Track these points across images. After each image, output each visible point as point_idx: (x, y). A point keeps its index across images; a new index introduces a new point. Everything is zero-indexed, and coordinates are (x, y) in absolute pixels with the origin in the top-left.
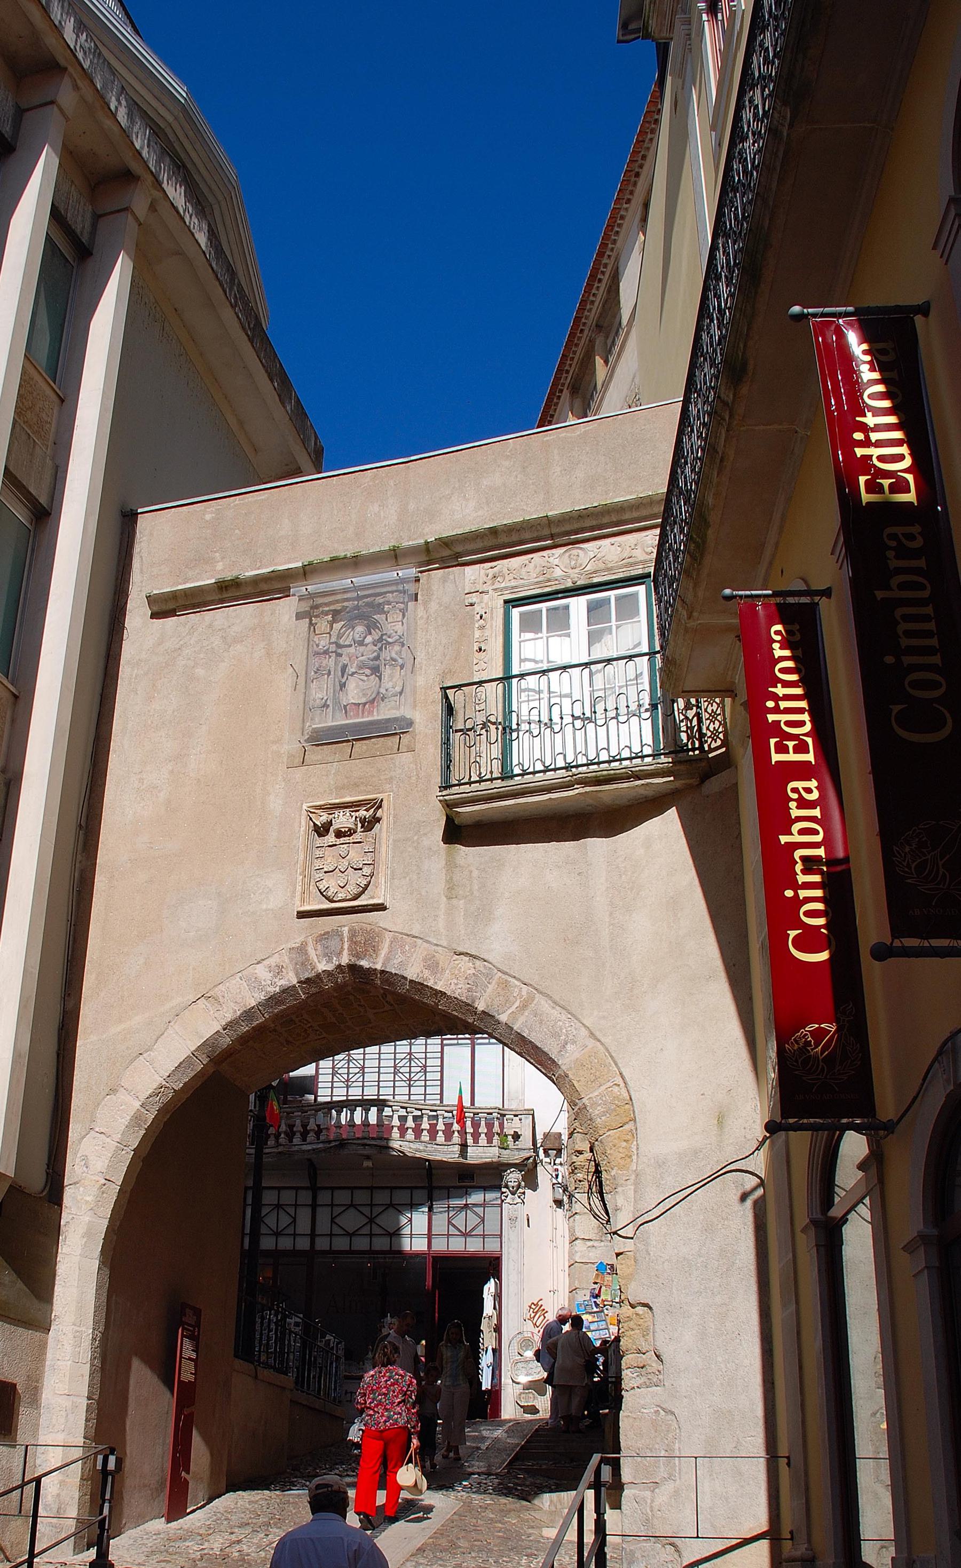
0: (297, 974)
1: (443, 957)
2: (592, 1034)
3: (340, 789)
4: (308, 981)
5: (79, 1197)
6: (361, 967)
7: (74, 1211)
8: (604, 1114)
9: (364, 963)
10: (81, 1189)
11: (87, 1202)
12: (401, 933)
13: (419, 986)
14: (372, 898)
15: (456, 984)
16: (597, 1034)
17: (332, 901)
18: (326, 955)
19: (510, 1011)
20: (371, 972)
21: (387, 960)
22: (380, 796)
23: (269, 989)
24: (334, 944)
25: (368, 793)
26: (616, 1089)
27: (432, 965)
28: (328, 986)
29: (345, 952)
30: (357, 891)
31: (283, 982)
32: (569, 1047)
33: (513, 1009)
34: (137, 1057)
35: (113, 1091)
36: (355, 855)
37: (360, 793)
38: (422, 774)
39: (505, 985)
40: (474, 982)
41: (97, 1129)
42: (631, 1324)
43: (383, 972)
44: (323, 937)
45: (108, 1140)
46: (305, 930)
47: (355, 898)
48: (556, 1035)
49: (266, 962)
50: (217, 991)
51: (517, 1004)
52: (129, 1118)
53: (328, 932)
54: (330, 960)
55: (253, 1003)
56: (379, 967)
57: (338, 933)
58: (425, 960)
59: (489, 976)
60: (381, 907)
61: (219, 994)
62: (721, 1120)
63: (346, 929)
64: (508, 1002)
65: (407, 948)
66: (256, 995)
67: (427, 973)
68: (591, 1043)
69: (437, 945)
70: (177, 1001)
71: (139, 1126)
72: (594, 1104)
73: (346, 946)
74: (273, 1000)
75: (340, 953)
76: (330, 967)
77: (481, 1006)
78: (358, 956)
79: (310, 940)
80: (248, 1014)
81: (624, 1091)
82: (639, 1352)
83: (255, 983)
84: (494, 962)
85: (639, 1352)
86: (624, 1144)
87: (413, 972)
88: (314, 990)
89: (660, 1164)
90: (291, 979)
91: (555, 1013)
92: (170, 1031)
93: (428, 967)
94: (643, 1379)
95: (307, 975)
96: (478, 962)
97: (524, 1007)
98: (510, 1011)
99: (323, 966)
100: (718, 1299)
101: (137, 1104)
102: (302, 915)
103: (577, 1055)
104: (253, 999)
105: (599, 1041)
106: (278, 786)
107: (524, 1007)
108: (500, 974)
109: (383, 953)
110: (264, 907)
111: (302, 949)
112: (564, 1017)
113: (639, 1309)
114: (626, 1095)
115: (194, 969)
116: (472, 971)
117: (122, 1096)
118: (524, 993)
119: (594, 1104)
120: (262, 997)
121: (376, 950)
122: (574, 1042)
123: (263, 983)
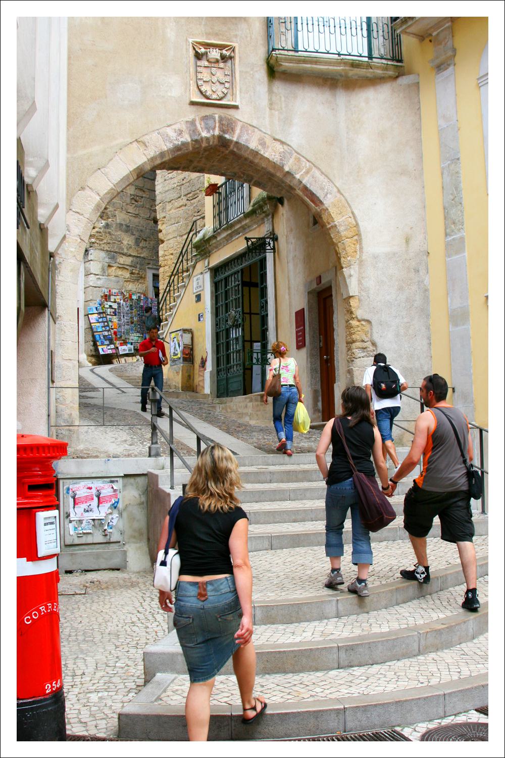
0: (191, 136)
1: (268, 140)
2: (339, 191)
3: (208, 35)
4: (196, 141)
5: (66, 249)
6: (225, 138)
7: (63, 256)
8: (346, 230)
9: (227, 136)
10: (67, 244)
11: (72, 252)
12: (247, 123)
13: (256, 153)
14: (229, 101)
15: (275, 155)
16: (342, 191)
17: (208, 98)
18: (206, 128)
19: (300, 174)
20: (230, 141)
21: (239, 136)
22: (234, 44)
23: (175, 142)
24: (211, 122)
25: (224, 41)
26: (350, 219)
27: (263, 143)
28: (204, 145)
29: (217, 129)
30: (222, 95)
31: (183, 140)
32: (329, 196)
33: (302, 173)
34: (97, 170)
35: (83, 188)
36: (219, 75)
37: (220, 40)
38: (253, 37)
39: (299, 160)
40: (283, 155)
41: (74, 210)
42: (359, 329)
43: (237, 143)
44: (205, 118)
45: (81, 217)
46: (192, 114)
47: (220, 99)
48: (322, 189)
49: (173, 127)
50: (146, 139)
51: (304, 170)
52: (94, 205)
53: (207, 116)
54: (209, 132)
55: (166, 149)
56: (235, 139)
57: (212, 117)
58: (259, 140)
59: (291, 154)
60: (236, 107)
61: (146, 141)
62: (407, 241)
63: (217, 117)
64: (300, 169)
65: (250, 132)
66: (167, 144)
67: (260, 147)
68: (338, 195)
69: (265, 133)
70: (120, 141)
71: (98, 210)
72: (340, 225)
73: (217, 125)
74: (178, 148)
75: (214, 129)
76: (208, 135)
77: (287, 169)
78: (224, 132)
79: (197, 119)
80: (162, 154)
81: (353, 220)
82: (363, 341)
83: (166, 137)
84: (294, 147)
85: (363, 341)
86: (353, 246)
87: (253, 145)
88: (197, 146)
89: (375, 257)
90: (187, 138)
91: (322, 178)
92: (117, 158)
93: (261, 144)
94: (365, 354)
95: (196, 137)
96: (285, 147)
97: (307, 172)
98: (300, 174)
99: (204, 134)
100: (405, 320)
101: (98, 198)
102: (193, 103)
103: (332, 200)
104: (166, 146)
105: (342, 195)
106: (171, 24)
107: (307, 172)
108: (296, 154)
109: (238, 131)
110: (169, 94)
111: (193, 123)
112: (326, 180)
113: (363, 323)
114: (354, 223)
115: (129, 123)
116: (282, 150)
117: (88, 192)
118: (307, 165)
119: (340, 225)
120: (170, 146)
121: (233, 130)
122: (331, 194)
123: (171, 138)
